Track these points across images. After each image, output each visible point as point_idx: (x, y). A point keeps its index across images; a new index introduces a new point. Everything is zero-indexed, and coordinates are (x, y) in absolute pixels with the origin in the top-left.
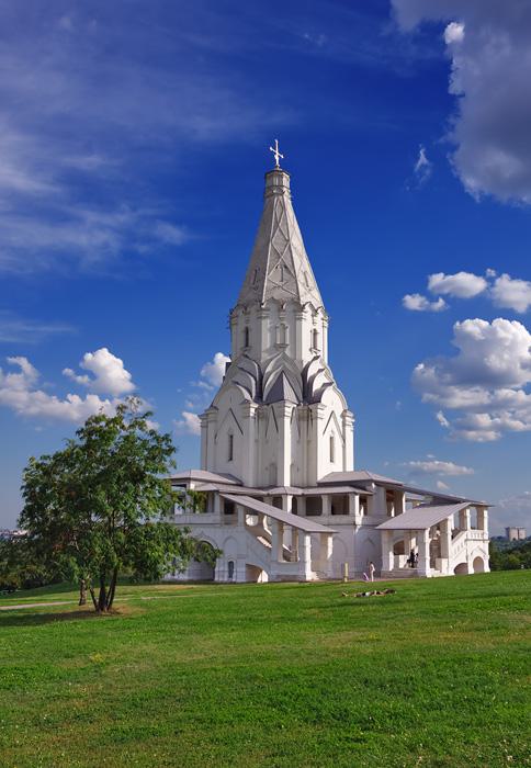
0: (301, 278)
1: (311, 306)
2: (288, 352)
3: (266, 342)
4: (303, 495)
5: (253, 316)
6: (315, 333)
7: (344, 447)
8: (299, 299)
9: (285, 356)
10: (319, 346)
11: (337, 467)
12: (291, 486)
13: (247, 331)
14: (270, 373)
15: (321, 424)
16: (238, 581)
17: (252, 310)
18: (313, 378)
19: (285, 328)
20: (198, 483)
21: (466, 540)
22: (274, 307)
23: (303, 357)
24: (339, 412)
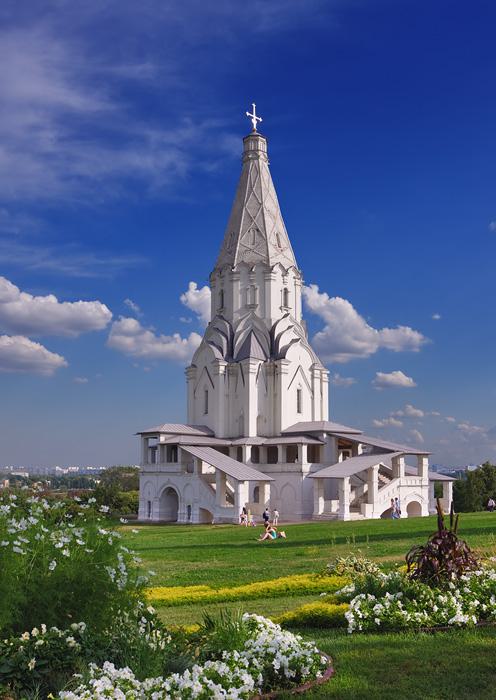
0: (272, 240)
1: (281, 266)
2: (257, 312)
3: (238, 303)
4: (263, 445)
5: (227, 278)
6: (286, 291)
7: (321, 401)
8: (268, 261)
9: (254, 317)
10: (291, 303)
11: (306, 417)
12: (258, 435)
13: (222, 294)
14: (240, 333)
15: (285, 380)
16: (194, 522)
17: (226, 273)
18: (280, 335)
19: (255, 289)
21: (399, 487)
22: (244, 271)
23: (272, 316)
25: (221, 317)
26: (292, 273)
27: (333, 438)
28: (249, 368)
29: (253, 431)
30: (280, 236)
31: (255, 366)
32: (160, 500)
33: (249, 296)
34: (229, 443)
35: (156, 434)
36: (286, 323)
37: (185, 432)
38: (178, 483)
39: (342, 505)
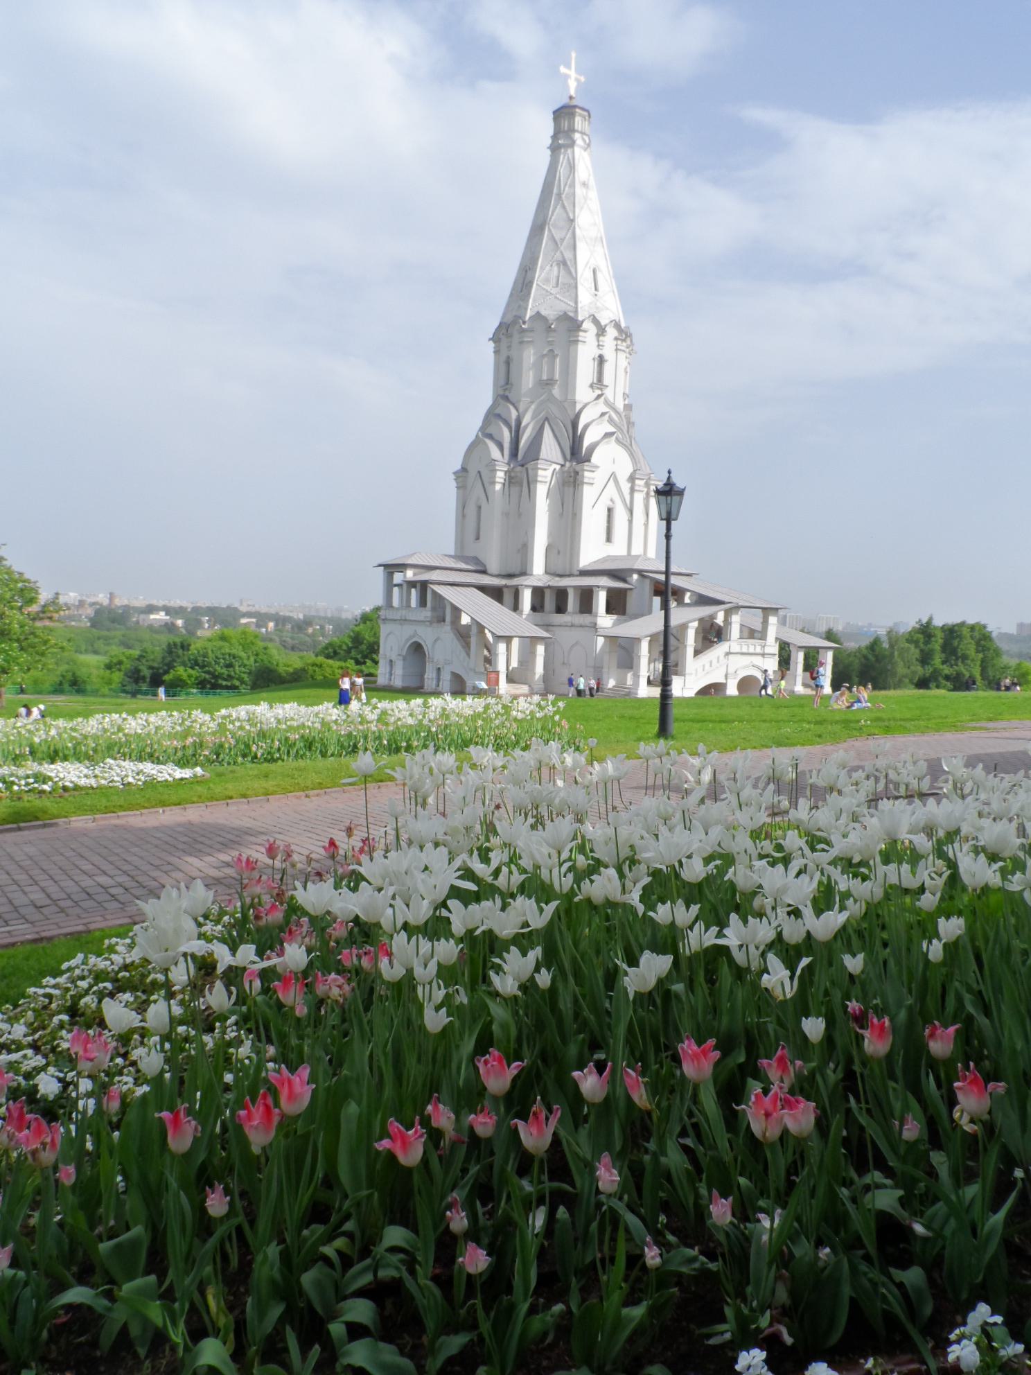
1: (596, 321)
2: (556, 391)
3: (528, 380)
6: (601, 360)
7: (646, 525)
8: (576, 312)
9: (551, 398)
10: (608, 379)
11: (618, 549)
12: (546, 572)
13: (508, 362)
14: (526, 427)
18: (586, 427)
19: (555, 357)
20: (417, 570)
21: (728, 654)
24: (623, 478)
25: (506, 398)
26: (612, 332)
27: (647, 582)
28: (536, 475)
29: (538, 566)
30: (599, 275)
31: (546, 474)
32: (404, 659)
33: (545, 368)
34: (503, 582)
35: (402, 567)
36: (602, 407)
37: (448, 565)
38: (426, 636)
39: (637, 676)
